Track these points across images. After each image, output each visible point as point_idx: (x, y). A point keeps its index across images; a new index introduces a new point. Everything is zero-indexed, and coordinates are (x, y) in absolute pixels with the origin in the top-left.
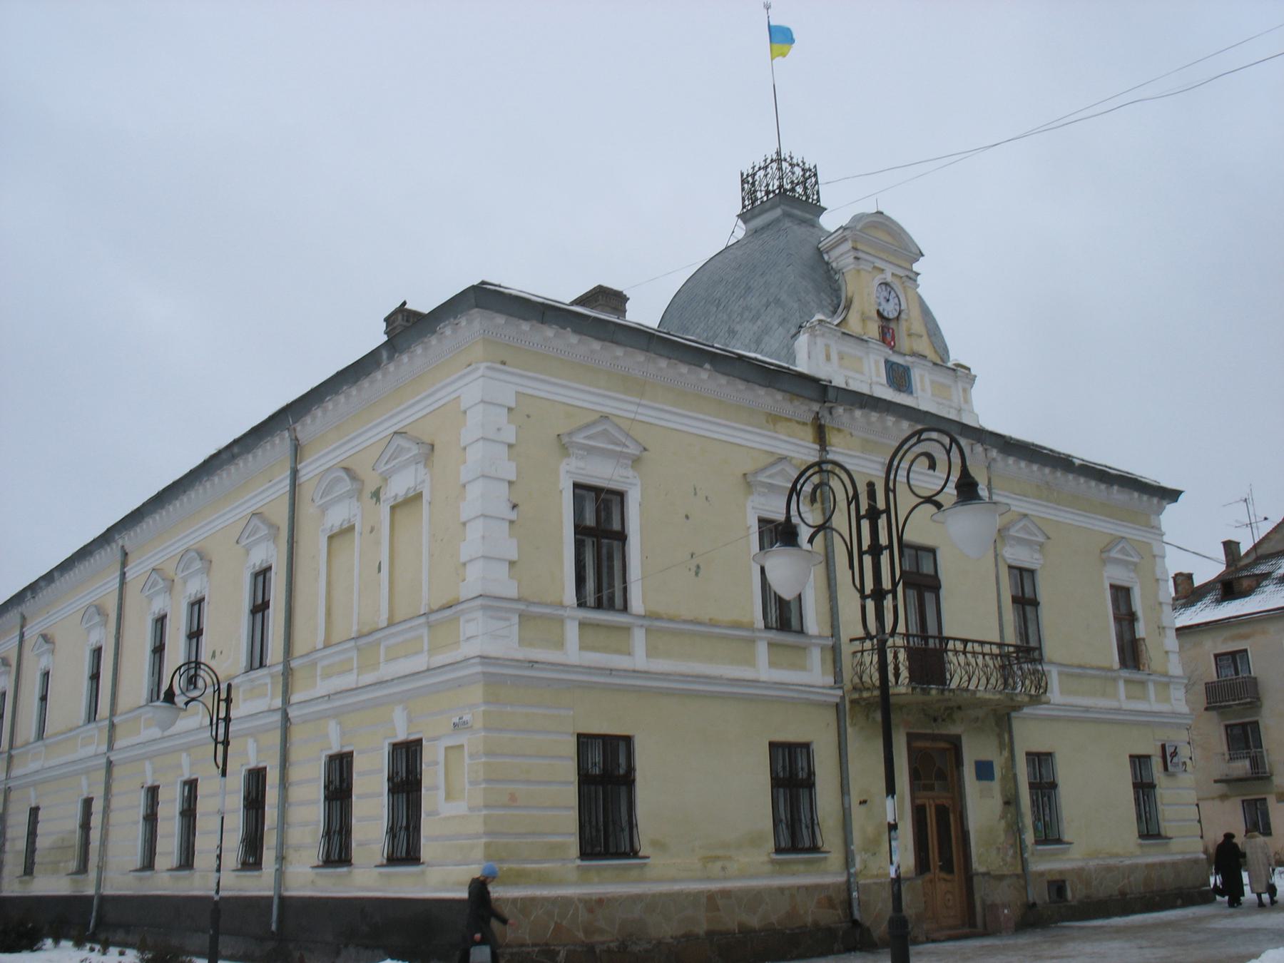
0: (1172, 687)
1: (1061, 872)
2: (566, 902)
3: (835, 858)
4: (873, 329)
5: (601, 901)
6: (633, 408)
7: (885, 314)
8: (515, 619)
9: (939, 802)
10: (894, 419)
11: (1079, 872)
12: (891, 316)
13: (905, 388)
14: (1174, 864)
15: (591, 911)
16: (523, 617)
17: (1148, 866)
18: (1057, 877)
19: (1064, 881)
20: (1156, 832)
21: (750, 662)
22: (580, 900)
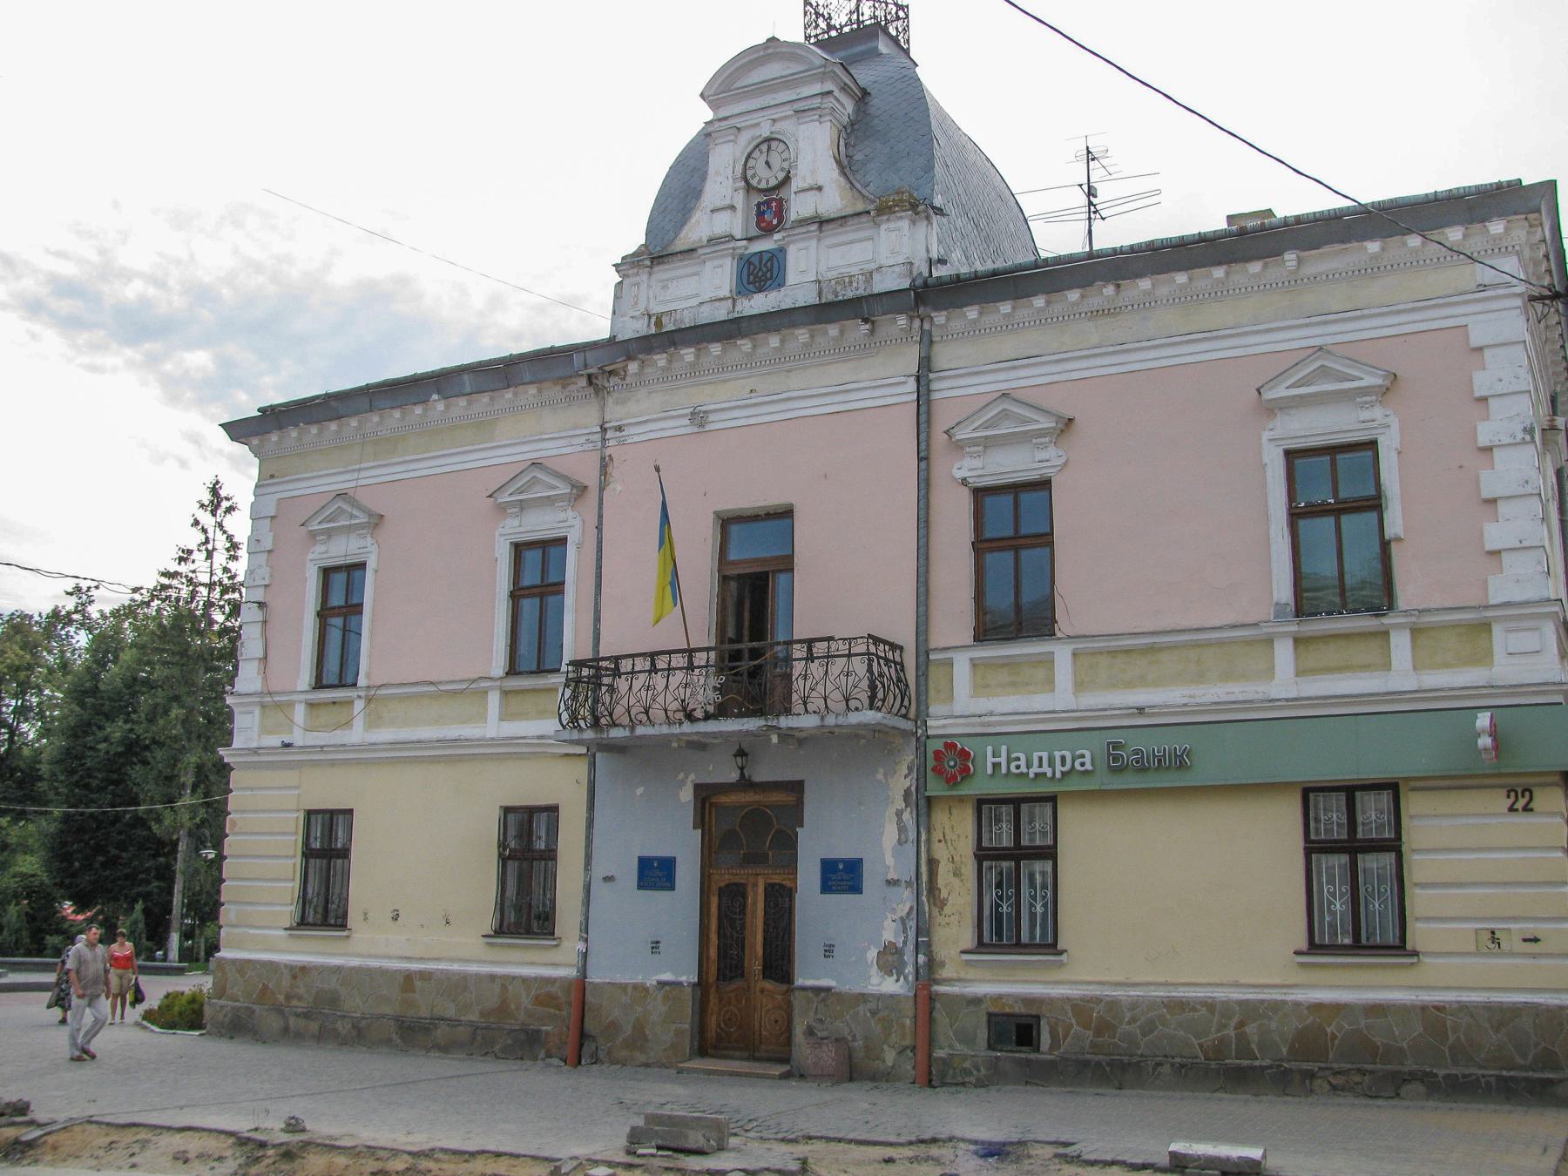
0: (1497, 630)
1: (1028, 1001)
2: (273, 966)
3: (571, 946)
4: (734, 224)
5: (304, 969)
6: (355, 475)
7: (763, 185)
8: (257, 711)
9: (776, 879)
10: (693, 350)
11: (1081, 1008)
12: (773, 183)
13: (769, 282)
14: (1433, 1016)
15: (294, 977)
16: (263, 706)
17: (1317, 1007)
18: (1019, 1009)
19: (1038, 1018)
20: (1392, 939)
21: (482, 717)
22: (286, 966)
